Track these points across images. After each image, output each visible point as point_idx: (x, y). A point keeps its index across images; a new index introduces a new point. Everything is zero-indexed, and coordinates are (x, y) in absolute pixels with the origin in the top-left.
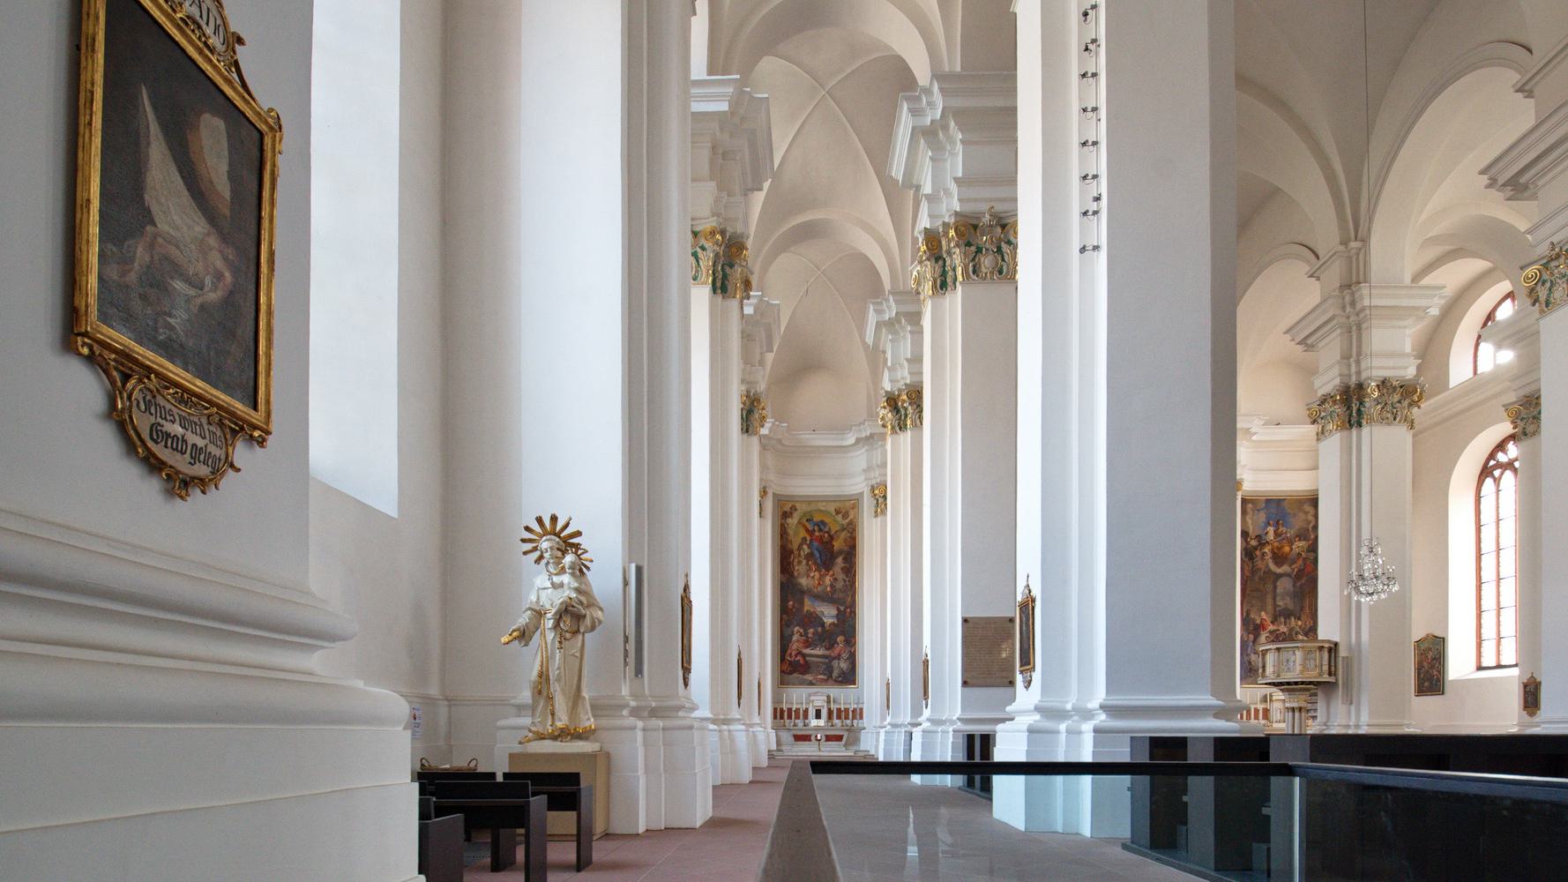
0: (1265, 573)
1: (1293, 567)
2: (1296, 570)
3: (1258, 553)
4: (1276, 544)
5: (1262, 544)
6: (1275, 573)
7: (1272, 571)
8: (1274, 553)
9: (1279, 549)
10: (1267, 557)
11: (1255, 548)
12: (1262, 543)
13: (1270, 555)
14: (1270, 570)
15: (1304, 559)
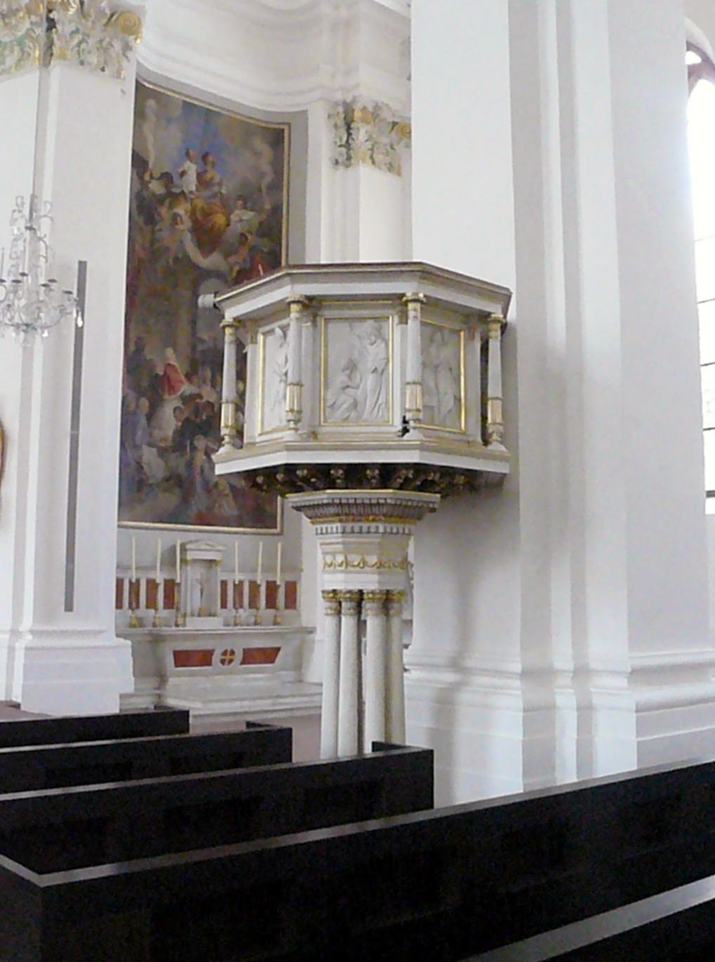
0: (176, 259)
1: (232, 259)
2: (236, 268)
3: (164, 211)
4: (200, 203)
5: (174, 197)
6: (195, 267)
7: (190, 260)
8: (193, 214)
9: (207, 214)
10: (180, 227)
11: (160, 200)
12: (174, 197)
13: (187, 224)
14: (187, 257)
15: (252, 249)
